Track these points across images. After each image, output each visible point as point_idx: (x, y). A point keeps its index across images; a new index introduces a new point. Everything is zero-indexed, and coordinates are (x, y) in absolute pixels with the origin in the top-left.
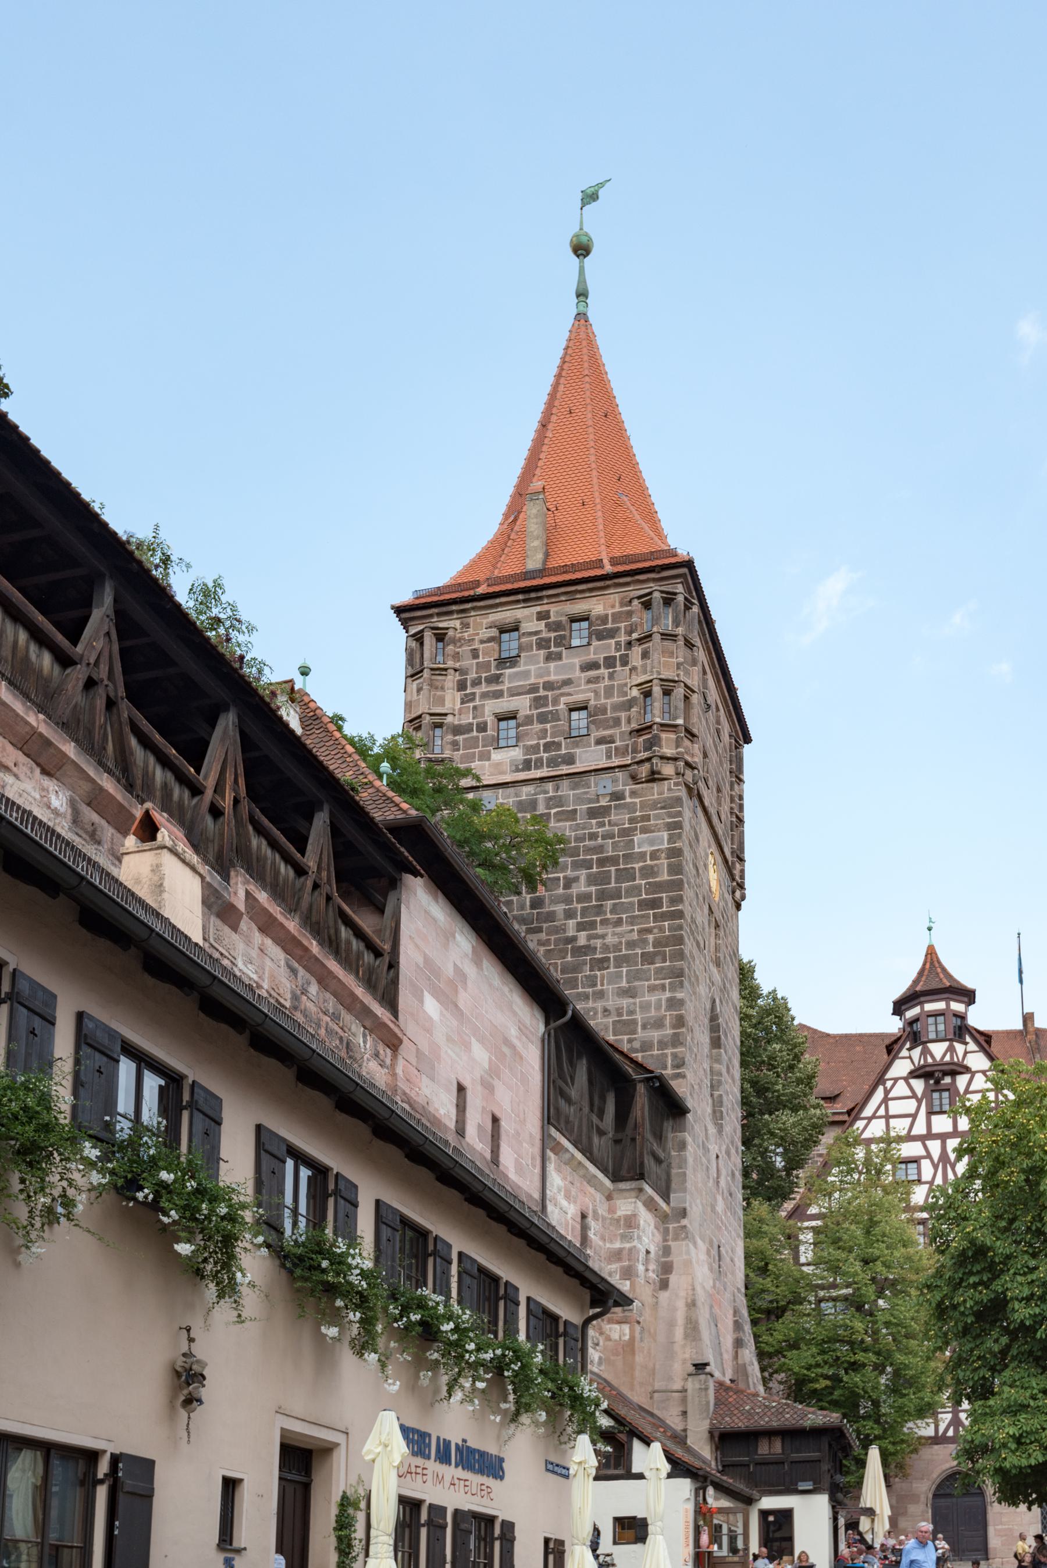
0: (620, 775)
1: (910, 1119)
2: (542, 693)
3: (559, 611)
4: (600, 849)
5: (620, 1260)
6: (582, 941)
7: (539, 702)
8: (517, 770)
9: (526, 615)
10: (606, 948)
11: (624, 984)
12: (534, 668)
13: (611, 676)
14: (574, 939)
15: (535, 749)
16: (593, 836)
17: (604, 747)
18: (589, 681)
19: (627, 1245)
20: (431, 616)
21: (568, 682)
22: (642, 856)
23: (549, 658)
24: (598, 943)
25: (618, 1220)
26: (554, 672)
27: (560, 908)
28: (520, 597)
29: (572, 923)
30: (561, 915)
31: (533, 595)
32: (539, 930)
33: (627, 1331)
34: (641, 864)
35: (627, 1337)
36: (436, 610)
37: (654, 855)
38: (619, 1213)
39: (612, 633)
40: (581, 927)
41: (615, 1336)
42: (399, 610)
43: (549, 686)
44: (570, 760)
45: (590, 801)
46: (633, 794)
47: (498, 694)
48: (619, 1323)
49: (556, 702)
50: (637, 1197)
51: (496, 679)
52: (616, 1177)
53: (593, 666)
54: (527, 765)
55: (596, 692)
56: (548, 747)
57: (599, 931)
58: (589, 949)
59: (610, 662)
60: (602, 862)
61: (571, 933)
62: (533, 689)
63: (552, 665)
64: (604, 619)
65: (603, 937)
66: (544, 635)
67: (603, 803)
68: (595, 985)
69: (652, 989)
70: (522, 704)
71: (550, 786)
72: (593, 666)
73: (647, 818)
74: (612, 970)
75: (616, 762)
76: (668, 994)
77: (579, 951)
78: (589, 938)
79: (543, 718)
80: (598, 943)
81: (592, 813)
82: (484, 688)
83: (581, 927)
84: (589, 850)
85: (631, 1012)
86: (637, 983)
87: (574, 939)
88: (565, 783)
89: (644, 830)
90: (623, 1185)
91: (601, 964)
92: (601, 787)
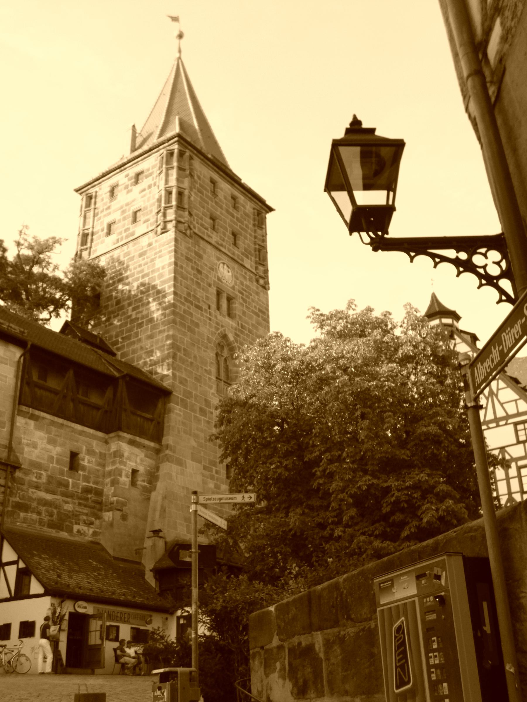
0: (151, 234)
1: (500, 387)
2: (124, 208)
3: (132, 171)
4: (142, 271)
5: (110, 476)
6: (134, 317)
7: (123, 212)
8: (114, 244)
9: (120, 178)
10: (143, 317)
11: (149, 333)
12: (122, 197)
13: (150, 193)
14: (131, 316)
15: (121, 233)
16: (140, 266)
17: (145, 224)
18: (142, 197)
19: (114, 467)
20: (88, 189)
21: (134, 201)
22: (158, 269)
23: (128, 192)
24: (140, 316)
25: (111, 454)
26: (130, 197)
27: (126, 303)
28: (118, 170)
29: (130, 308)
30: (126, 306)
31: (122, 168)
32: (118, 315)
33: (111, 516)
34: (158, 273)
35: (111, 519)
36: (89, 186)
37: (163, 268)
38: (112, 450)
39: (151, 174)
40: (134, 309)
41: (106, 519)
42: (77, 191)
43: (127, 204)
44: (133, 234)
45: (140, 250)
46: (156, 241)
47: (109, 214)
48: (108, 511)
49: (129, 210)
50: (119, 440)
51: (109, 208)
52: (107, 431)
53: (144, 190)
54: (118, 241)
55: (144, 201)
56: (126, 231)
57: (141, 309)
58: (138, 319)
59: (150, 187)
60: (143, 277)
61: (129, 314)
62: (122, 207)
63: (130, 194)
64: (148, 170)
65: (141, 312)
66: (127, 184)
67: (145, 249)
68: (138, 336)
69: (160, 332)
70: (116, 216)
71: (125, 247)
72: (144, 190)
73: (161, 251)
74: (145, 327)
75: (150, 229)
76: (166, 334)
77: (133, 321)
78: (137, 313)
79: (124, 219)
80: (140, 316)
81: (141, 255)
82: (105, 213)
83: (134, 309)
84: (139, 272)
85: (152, 346)
86: (154, 331)
87: (131, 316)
88: (131, 244)
89: (160, 257)
90: (112, 435)
91: (140, 325)
92: (144, 241)
